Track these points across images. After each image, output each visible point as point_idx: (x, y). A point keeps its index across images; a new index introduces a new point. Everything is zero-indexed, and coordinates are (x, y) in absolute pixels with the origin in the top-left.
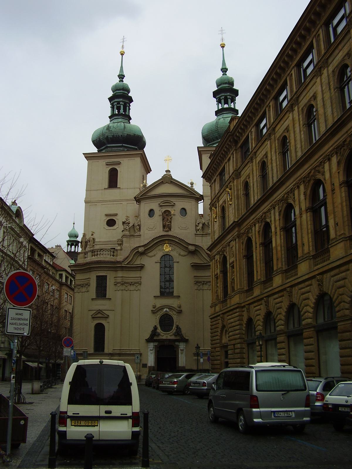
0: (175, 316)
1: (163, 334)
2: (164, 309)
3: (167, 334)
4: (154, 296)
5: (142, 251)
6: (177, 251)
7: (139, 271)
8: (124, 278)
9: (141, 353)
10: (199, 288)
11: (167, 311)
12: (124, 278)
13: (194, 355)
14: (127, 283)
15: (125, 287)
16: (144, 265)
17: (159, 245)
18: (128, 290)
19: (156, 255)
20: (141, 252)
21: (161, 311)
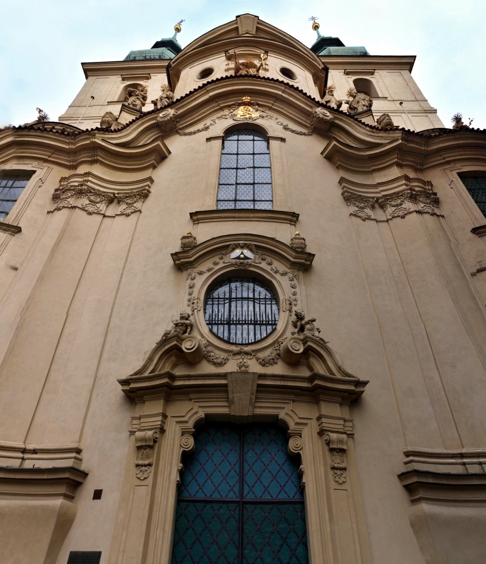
0: (286, 278)
1: (224, 355)
2: (234, 249)
3: (247, 353)
4: (192, 215)
5: (169, 118)
6: (278, 121)
7: (151, 169)
8: (90, 178)
9: (83, 467)
10: (362, 215)
11: (246, 258)
12: (90, 178)
13: (409, 489)
14: (98, 194)
15: (88, 202)
16: (170, 153)
17: (222, 109)
18: (98, 213)
19: (211, 127)
20: (166, 119)
21: (216, 259)
